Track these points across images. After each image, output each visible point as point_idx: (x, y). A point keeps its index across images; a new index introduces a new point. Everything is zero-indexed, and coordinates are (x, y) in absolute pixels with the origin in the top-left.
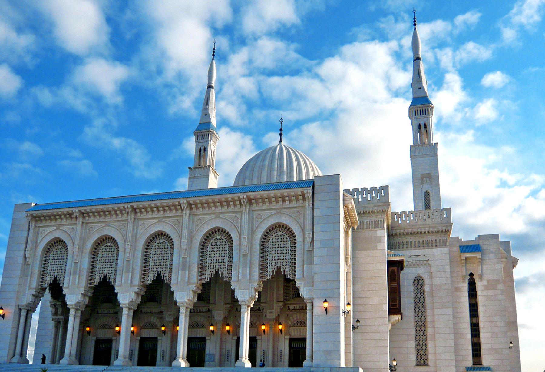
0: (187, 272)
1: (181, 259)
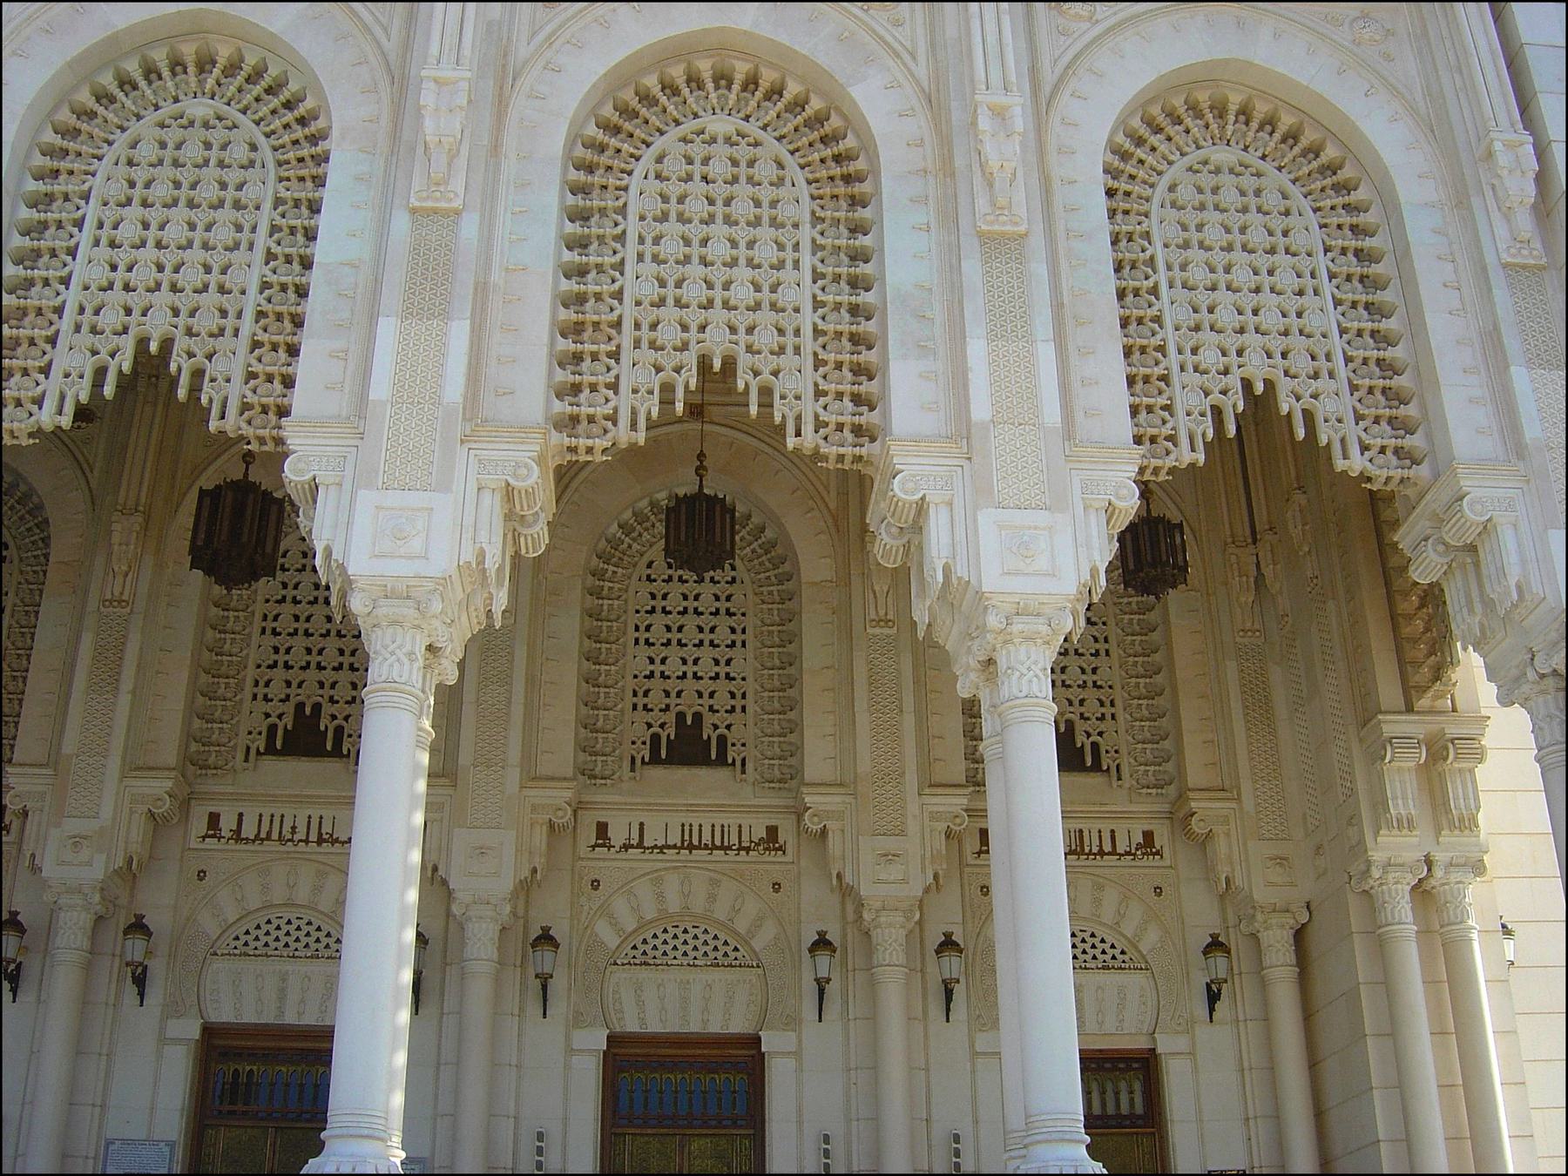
0: (459, 333)
1: (401, 224)
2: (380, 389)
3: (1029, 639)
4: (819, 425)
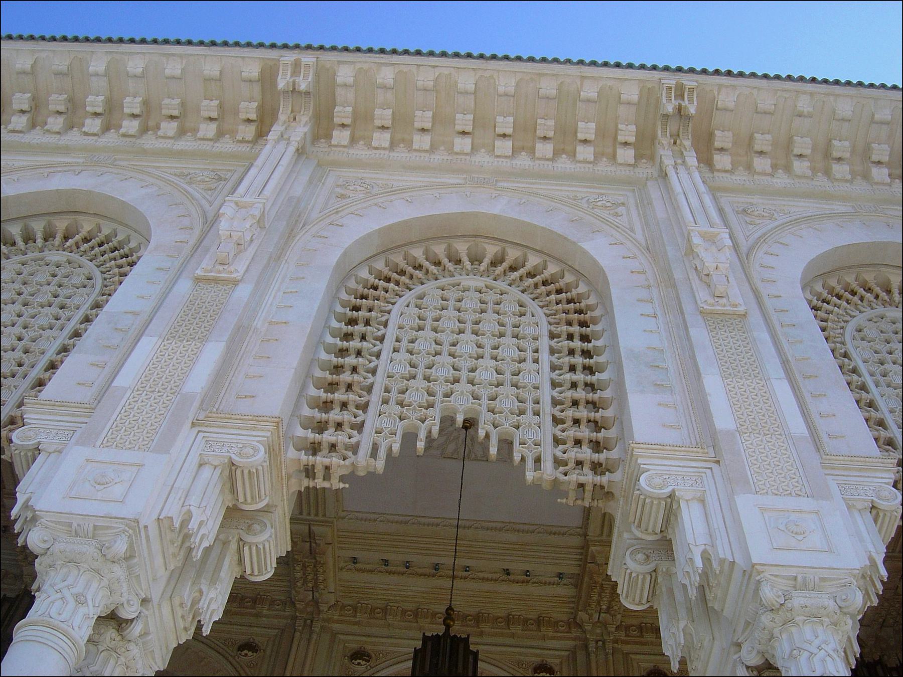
1: (184, 286)
2: (126, 379)
3: (814, 616)
4: (558, 463)
